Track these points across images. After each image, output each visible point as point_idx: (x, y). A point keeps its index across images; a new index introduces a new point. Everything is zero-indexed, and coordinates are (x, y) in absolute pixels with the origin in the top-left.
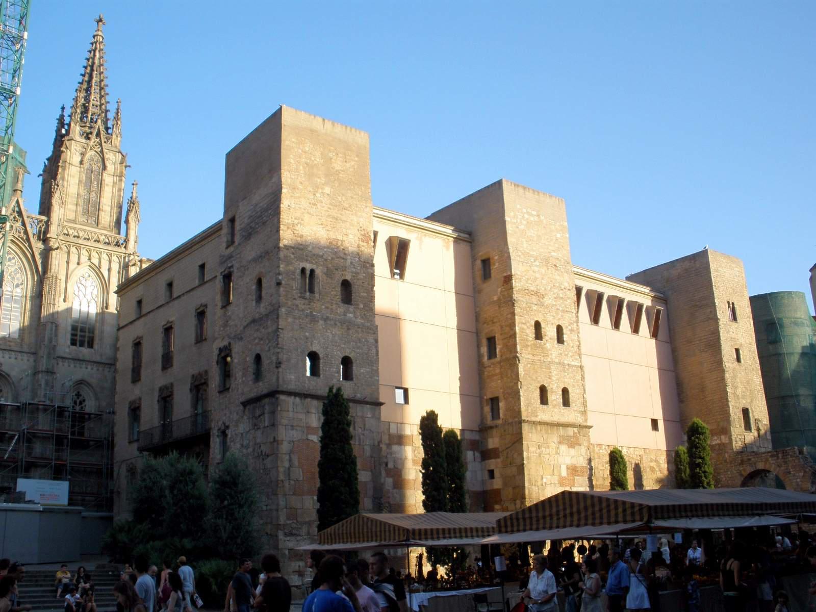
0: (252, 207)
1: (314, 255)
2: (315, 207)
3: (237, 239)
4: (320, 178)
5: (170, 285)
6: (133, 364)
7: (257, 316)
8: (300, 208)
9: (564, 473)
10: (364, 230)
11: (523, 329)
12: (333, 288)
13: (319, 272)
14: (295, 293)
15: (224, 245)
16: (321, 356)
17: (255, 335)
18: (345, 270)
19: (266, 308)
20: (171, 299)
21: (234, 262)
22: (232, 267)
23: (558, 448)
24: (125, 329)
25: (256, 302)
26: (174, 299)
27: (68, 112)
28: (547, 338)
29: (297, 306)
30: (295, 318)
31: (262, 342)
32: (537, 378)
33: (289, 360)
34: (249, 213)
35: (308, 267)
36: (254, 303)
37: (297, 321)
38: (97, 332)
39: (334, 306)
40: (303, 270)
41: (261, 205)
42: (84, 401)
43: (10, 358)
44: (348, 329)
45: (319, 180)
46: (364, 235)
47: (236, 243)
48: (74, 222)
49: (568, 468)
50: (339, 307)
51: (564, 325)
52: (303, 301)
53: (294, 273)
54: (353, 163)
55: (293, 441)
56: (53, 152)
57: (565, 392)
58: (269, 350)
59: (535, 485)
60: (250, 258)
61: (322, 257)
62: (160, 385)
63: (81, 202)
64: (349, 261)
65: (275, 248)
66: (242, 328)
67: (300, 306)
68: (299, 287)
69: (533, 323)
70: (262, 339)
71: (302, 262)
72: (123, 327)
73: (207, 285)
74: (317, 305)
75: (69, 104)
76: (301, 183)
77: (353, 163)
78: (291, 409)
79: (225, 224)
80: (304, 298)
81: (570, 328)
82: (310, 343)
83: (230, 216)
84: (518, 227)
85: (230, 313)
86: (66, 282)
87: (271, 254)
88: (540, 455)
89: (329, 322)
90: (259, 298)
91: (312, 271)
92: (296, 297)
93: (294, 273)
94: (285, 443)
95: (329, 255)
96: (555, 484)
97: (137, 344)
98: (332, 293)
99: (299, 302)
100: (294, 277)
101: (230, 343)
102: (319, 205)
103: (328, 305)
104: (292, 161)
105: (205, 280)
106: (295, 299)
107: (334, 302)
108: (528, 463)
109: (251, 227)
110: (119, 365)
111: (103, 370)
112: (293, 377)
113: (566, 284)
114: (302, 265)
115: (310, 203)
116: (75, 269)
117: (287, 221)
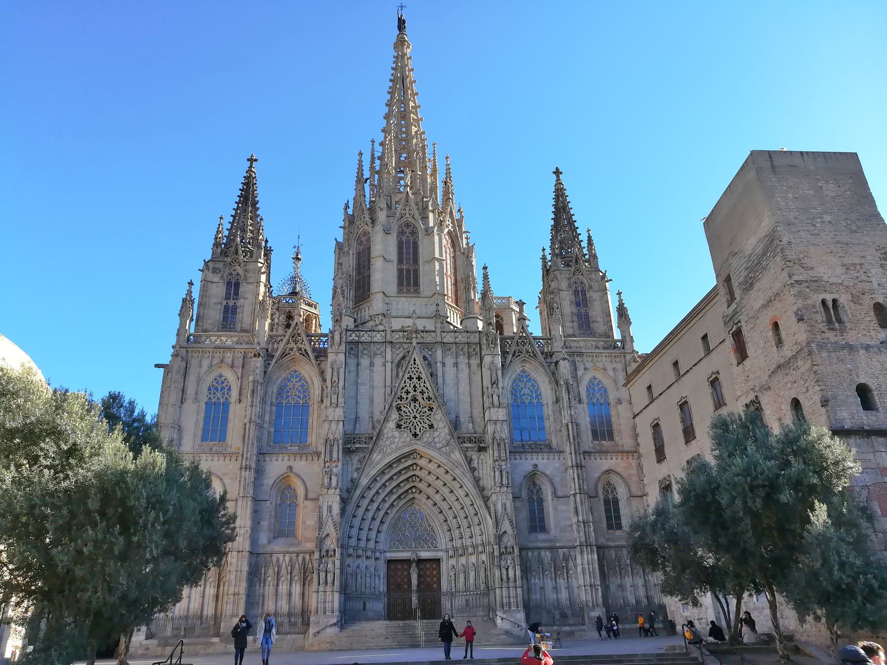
0: (746, 259)
1: (833, 284)
2: (818, 237)
3: (738, 293)
4: (814, 208)
5: (676, 364)
6: (655, 445)
7: (782, 361)
8: (802, 242)
10: (883, 248)
12: (865, 314)
13: (843, 299)
14: (823, 326)
15: (725, 305)
16: (873, 387)
17: (786, 380)
18: (875, 294)
19: (791, 350)
20: (679, 376)
21: (740, 317)
22: (739, 321)
24: (639, 416)
25: (777, 347)
26: (683, 376)
27: (548, 251)
29: (828, 339)
30: (829, 352)
31: (796, 385)
33: (835, 397)
34: (745, 265)
35: (829, 298)
36: (775, 349)
38: (614, 427)
39: (873, 333)
40: (824, 302)
41: (755, 253)
42: (615, 489)
43: (543, 459)
45: (814, 211)
47: (738, 299)
48: (574, 336)
50: (878, 332)
52: (833, 333)
53: (814, 306)
54: (847, 186)
55: (868, 487)
56: (544, 286)
58: (808, 390)
60: (758, 306)
62: (687, 459)
63: (575, 318)
65: (785, 286)
66: (766, 377)
67: (831, 338)
68: (824, 320)
70: (795, 382)
71: (821, 293)
72: (637, 414)
73: (713, 354)
75: (547, 244)
76: (796, 218)
77: (847, 186)
79: (721, 285)
80: (833, 329)
82: (855, 376)
83: (724, 276)
85: (749, 367)
86: (578, 387)
87: (782, 294)
89: (871, 350)
90: (779, 342)
91: (835, 301)
92: (824, 329)
93: (814, 306)
97: (656, 427)
98: (866, 319)
99: (831, 336)
100: (815, 310)
101: (757, 396)
102: (822, 235)
103: (864, 332)
105: (711, 349)
106: (823, 332)
107: (872, 328)
109: (750, 278)
110: (642, 450)
111: (628, 459)
112: (846, 414)
115: (811, 235)
116: (584, 374)
117: (791, 257)
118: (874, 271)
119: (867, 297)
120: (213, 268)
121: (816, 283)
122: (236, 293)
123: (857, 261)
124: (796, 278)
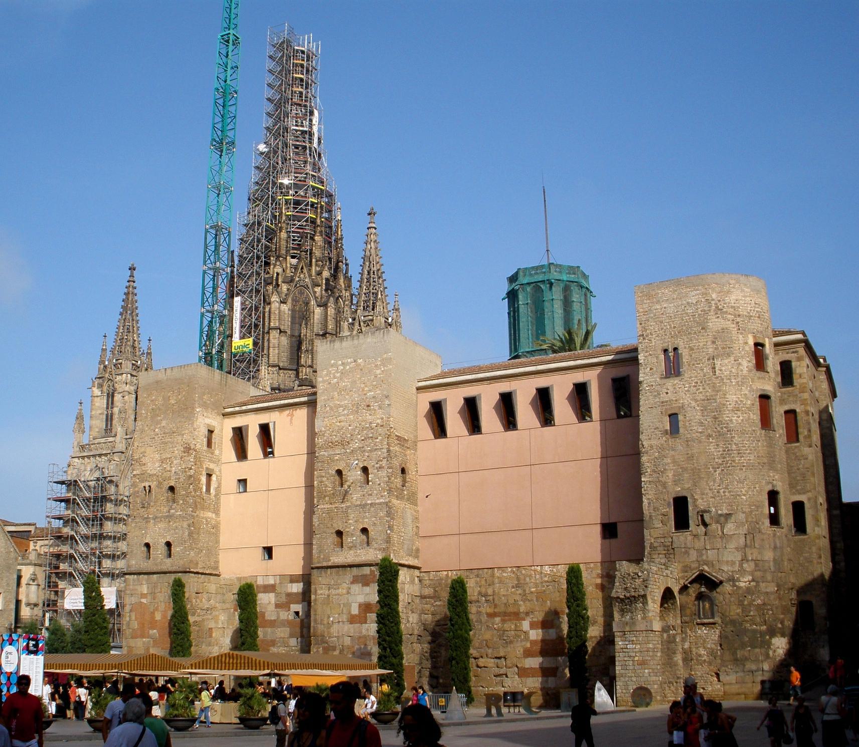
4: (160, 416)
9: (355, 610)
13: (154, 485)
23: (350, 588)
32: (332, 525)
35: (147, 484)
37: (138, 524)
40: (145, 487)
44: (170, 522)
45: (159, 418)
46: (186, 448)
49: (360, 606)
57: (364, 531)
59: (321, 624)
61: (155, 474)
64: (173, 472)
69: (334, 472)
74: (152, 510)
78: (132, 584)
81: (377, 466)
84: (330, 383)
88: (329, 596)
89: (157, 520)
94: (128, 606)
95: (160, 472)
96: (343, 622)
104: (143, 412)
108: (315, 604)
113: (379, 421)
114: (143, 485)
118: (175, 462)
120: (98, 383)
121: (143, 476)
122: (112, 403)
123: (169, 456)
124: (135, 473)
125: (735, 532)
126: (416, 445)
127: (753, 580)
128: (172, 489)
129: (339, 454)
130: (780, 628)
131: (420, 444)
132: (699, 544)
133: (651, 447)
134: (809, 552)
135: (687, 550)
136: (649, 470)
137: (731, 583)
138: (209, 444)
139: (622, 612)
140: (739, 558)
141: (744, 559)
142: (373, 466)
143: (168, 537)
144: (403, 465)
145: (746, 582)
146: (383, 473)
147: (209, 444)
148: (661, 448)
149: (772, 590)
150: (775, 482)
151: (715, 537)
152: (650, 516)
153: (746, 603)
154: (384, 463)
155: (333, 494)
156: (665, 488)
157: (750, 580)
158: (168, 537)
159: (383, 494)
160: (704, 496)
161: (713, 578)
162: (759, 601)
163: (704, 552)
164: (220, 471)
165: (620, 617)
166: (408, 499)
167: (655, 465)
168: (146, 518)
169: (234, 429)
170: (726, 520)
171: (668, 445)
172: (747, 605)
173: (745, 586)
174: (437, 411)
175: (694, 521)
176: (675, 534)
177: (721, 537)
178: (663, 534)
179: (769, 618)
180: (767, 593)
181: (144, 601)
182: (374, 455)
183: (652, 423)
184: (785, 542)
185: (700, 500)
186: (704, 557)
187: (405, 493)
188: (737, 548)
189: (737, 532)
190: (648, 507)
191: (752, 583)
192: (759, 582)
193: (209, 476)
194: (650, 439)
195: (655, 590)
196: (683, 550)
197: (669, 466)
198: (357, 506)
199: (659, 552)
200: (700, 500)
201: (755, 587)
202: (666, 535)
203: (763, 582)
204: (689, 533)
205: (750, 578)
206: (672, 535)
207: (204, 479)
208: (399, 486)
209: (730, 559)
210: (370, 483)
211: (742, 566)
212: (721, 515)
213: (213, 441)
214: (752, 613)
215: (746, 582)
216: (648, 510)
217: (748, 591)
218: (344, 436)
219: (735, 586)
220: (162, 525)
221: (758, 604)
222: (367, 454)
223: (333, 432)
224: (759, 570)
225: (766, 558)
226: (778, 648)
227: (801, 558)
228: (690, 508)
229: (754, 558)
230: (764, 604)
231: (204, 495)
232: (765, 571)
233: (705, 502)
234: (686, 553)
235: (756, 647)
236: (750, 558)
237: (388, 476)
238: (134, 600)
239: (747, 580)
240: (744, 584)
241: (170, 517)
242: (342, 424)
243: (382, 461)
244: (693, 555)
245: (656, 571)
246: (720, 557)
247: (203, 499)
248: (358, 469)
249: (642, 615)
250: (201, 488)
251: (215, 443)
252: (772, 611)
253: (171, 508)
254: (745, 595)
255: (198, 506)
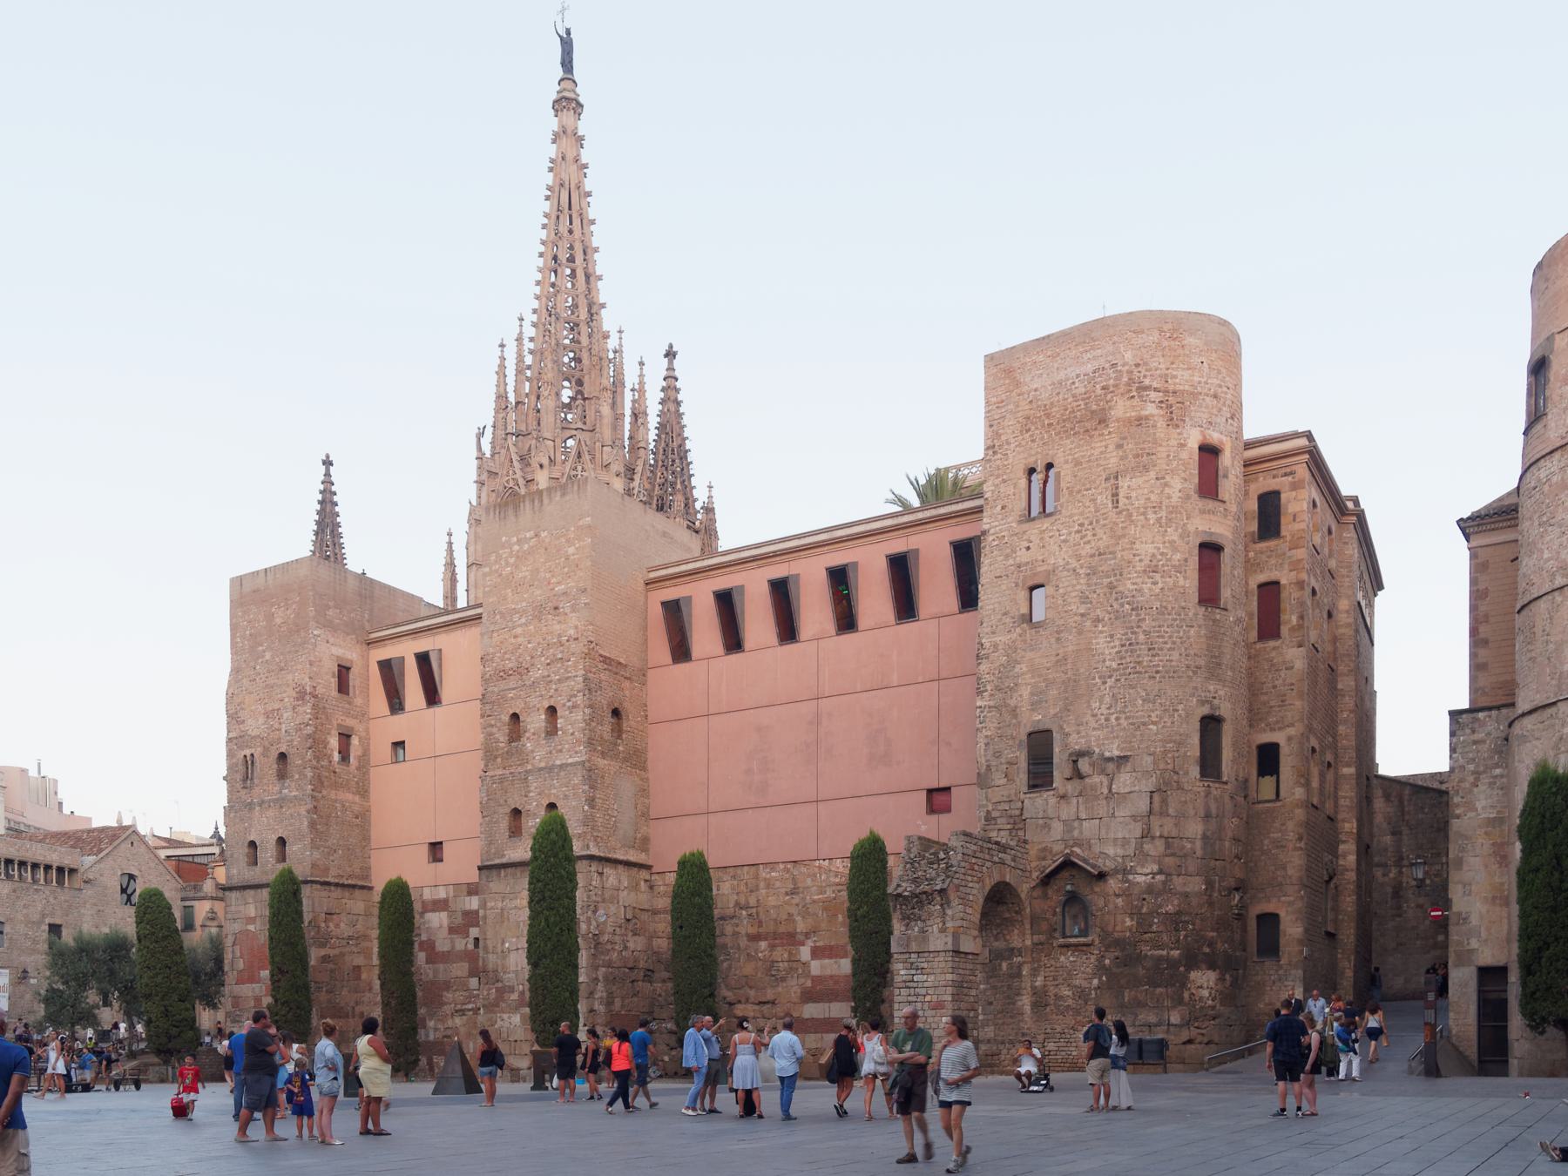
11: (491, 734)
13: (258, 751)
14: (239, 785)
28: (527, 735)
33: (232, 856)
44: (281, 807)
51: (558, 702)
74: (257, 790)
78: (233, 903)
81: (570, 704)
103: (265, 788)
119: (275, 747)
125: (1133, 789)
126: (644, 675)
127: (1161, 872)
128: (283, 757)
129: (513, 689)
130: (1205, 954)
131: (650, 673)
132: (1068, 811)
133: (996, 646)
134: (1281, 831)
135: (1047, 821)
136: (989, 688)
137: (1120, 877)
138: (343, 686)
139: (907, 919)
140: (1138, 834)
141: (1147, 835)
142: (564, 705)
143: (280, 831)
144: (616, 705)
145: (1146, 875)
146: (578, 716)
147: (343, 686)
148: (1012, 648)
149: (1196, 889)
150: (1216, 702)
151: (1097, 798)
152: (988, 766)
153: (1144, 910)
154: (579, 699)
155: (507, 753)
156: (1015, 716)
157: (1155, 871)
158: (280, 831)
159: (577, 749)
160: (1082, 728)
161: (1089, 868)
162: (1170, 908)
163: (1076, 824)
164: (367, 730)
165: (903, 928)
166: (625, 760)
167: (1000, 678)
168: (250, 804)
169: (380, 663)
170: (1118, 767)
171: (1025, 641)
172: (1145, 914)
173: (1145, 882)
174: (674, 611)
175: (1062, 773)
176: (1028, 796)
177: (1106, 798)
178: (1008, 797)
179: (1186, 936)
180: (1186, 895)
181: (251, 928)
182: (564, 687)
183: (999, 603)
184: (1229, 806)
185: (1075, 736)
186: (1076, 833)
187: (621, 748)
188: (1134, 817)
189: (1137, 788)
190: (986, 751)
191: (1158, 877)
192: (1170, 875)
193: (345, 737)
194: (993, 633)
195: (971, 885)
196: (1041, 822)
197: (1024, 679)
198: (541, 769)
199: (1001, 827)
200: (1075, 736)
201: (1164, 883)
202: (1014, 798)
203: (1179, 875)
204: (1052, 792)
205: (1155, 868)
206: (1022, 796)
207: (334, 742)
208: (607, 736)
209: (1120, 835)
210: (560, 733)
211: (1142, 847)
212: (1110, 759)
213: (351, 684)
214: (1154, 928)
215: (1146, 875)
216: (985, 756)
217: (1150, 889)
218: (521, 660)
219: (1127, 881)
220: (270, 813)
221: (1167, 913)
222: (554, 687)
223: (505, 653)
224: (1173, 855)
225: (1189, 834)
226: (1201, 987)
227: (1266, 842)
228: (1056, 750)
229: (1166, 835)
230: (1179, 913)
231: (336, 766)
232: (1185, 856)
233: (1083, 737)
234: (1047, 826)
235: (1159, 986)
236: (1158, 834)
237: (585, 720)
238: (237, 927)
239: (1149, 871)
240: (1144, 878)
241: (281, 802)
242: (520, 640)
243: (575, 696)
244: (1057, 829)
245: (975, 852)
246: (1103, 832)
247: (335, 772)
248: (542, 711)
249: (940, 925)
250: (331, 756)
251: (354, 687)
252: (1193, 924)
253: (283, 787)
254: (1145, 896)
255: (326, 783)
